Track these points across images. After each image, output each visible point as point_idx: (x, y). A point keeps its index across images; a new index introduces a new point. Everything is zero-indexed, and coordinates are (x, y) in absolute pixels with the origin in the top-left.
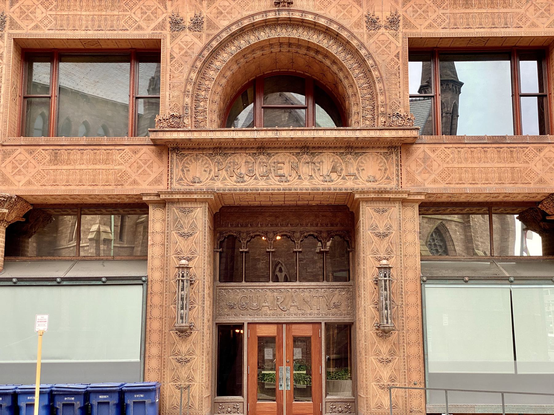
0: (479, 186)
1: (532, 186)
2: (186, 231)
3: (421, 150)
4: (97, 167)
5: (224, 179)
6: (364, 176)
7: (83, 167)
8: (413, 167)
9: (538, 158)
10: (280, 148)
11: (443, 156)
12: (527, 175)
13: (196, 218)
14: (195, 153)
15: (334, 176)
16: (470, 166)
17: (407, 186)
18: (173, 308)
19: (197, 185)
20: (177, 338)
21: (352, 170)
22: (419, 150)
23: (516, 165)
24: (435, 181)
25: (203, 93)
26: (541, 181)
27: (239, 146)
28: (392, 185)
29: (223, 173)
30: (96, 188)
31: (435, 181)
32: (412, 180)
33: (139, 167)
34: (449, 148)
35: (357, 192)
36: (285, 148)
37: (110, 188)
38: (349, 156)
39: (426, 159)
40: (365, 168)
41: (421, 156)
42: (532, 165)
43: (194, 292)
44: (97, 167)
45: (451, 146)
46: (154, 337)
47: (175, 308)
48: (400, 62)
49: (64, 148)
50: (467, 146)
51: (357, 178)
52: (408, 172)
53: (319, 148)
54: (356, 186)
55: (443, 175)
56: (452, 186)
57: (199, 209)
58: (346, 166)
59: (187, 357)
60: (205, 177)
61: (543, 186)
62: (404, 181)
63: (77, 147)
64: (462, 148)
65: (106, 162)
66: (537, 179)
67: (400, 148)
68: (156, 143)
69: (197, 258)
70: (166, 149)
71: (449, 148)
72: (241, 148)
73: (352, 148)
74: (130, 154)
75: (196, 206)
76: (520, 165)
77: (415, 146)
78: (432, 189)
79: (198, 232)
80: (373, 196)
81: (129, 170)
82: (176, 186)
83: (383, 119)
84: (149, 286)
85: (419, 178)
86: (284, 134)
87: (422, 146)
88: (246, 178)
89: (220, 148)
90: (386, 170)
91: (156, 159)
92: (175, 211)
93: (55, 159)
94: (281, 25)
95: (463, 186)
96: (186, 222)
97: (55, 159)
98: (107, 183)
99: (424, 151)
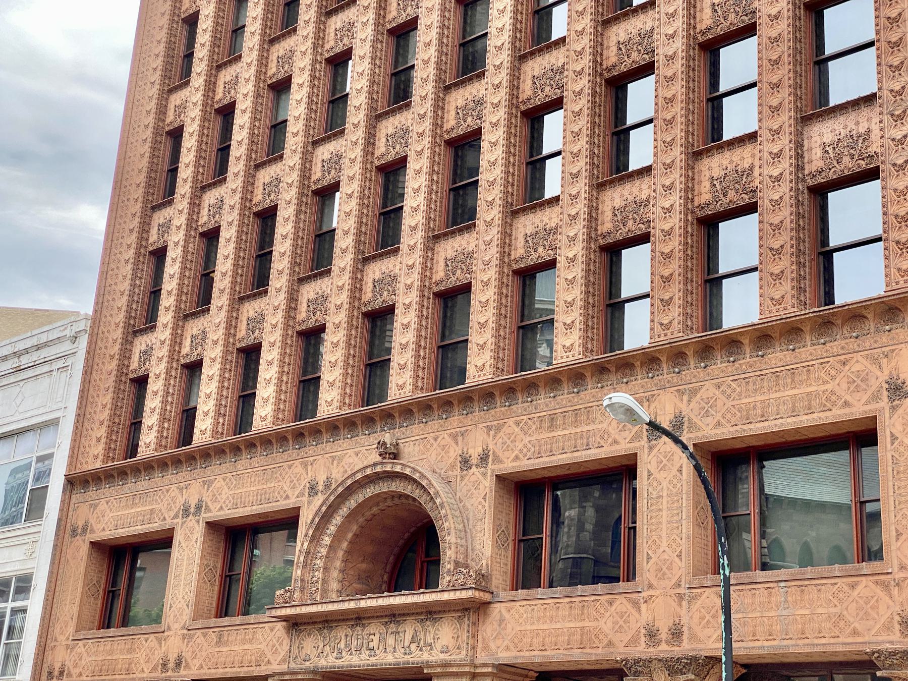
0: (548, 653)
1: (600, 651)
3: (497, 610)
4: (246, 647)
5: (327, 656)
6: (439, 646)
7: (236, 648)
8: (489, 631)
9: (609, 614)
10: (373, 617)
11: (517, 616)
12: (597, 636)
14: (309, 627)
15: (413, 646)
16: (542, 627)
17: (482, 658)
19: (307, 663)
21: (429, 640)
22: (497, 610)
23: (586, 624)
24: (508, 649)
25: (318, 562)
26: (610, 644)
27: (341, 618)
28: (462, 656)
29: (327, 648)
30: (242, 669)
31: (508, 649)
32: (486, 648)
33: (273, 646)
34: (523, 606)
35: (429, 667)
36: (377, 617)
37: (252, 669)
38: (428, 623)
39: (501, 621)
40: (440, 636)
41: (498, 618)
42: (601, 623)
44: (246, 647)
45: (524, 603)
48: (487, 505)
49: (226, 629)
50: (541, 602)
51: (431, 649)
52: (483, 638)
53: (404, 615)
54: (431, 659)
55: (516, 641)
56: (522, 654)
58: (425, 635)
60: (313, 654)
61: (611, 650)
62: (479, 650)
63: (235, 628)
64: (536, 605)
65: (251, 641)
66: (606, 641)
67: (474, 610)
68: (285, 619)
70: (295, 624)
71: (523, 606)
72: (343, 620)
73: (430, 613)
74: (269, 631)
76: (591, 624)
77: (493, 605)
78: (504, 658)
80: (438, 670)
82: (293, 666)
83: (448, 578)
85: (492, 646)
86: (364, 604)
87: (498, 605)
88: (344, 653)
89: (327, 621)
90: (458, 637)
91: (286, 637)
93: (219, 643)
94: (370, 482)
95: (533, 653)
97: (219, 643)
99: (500, 611)
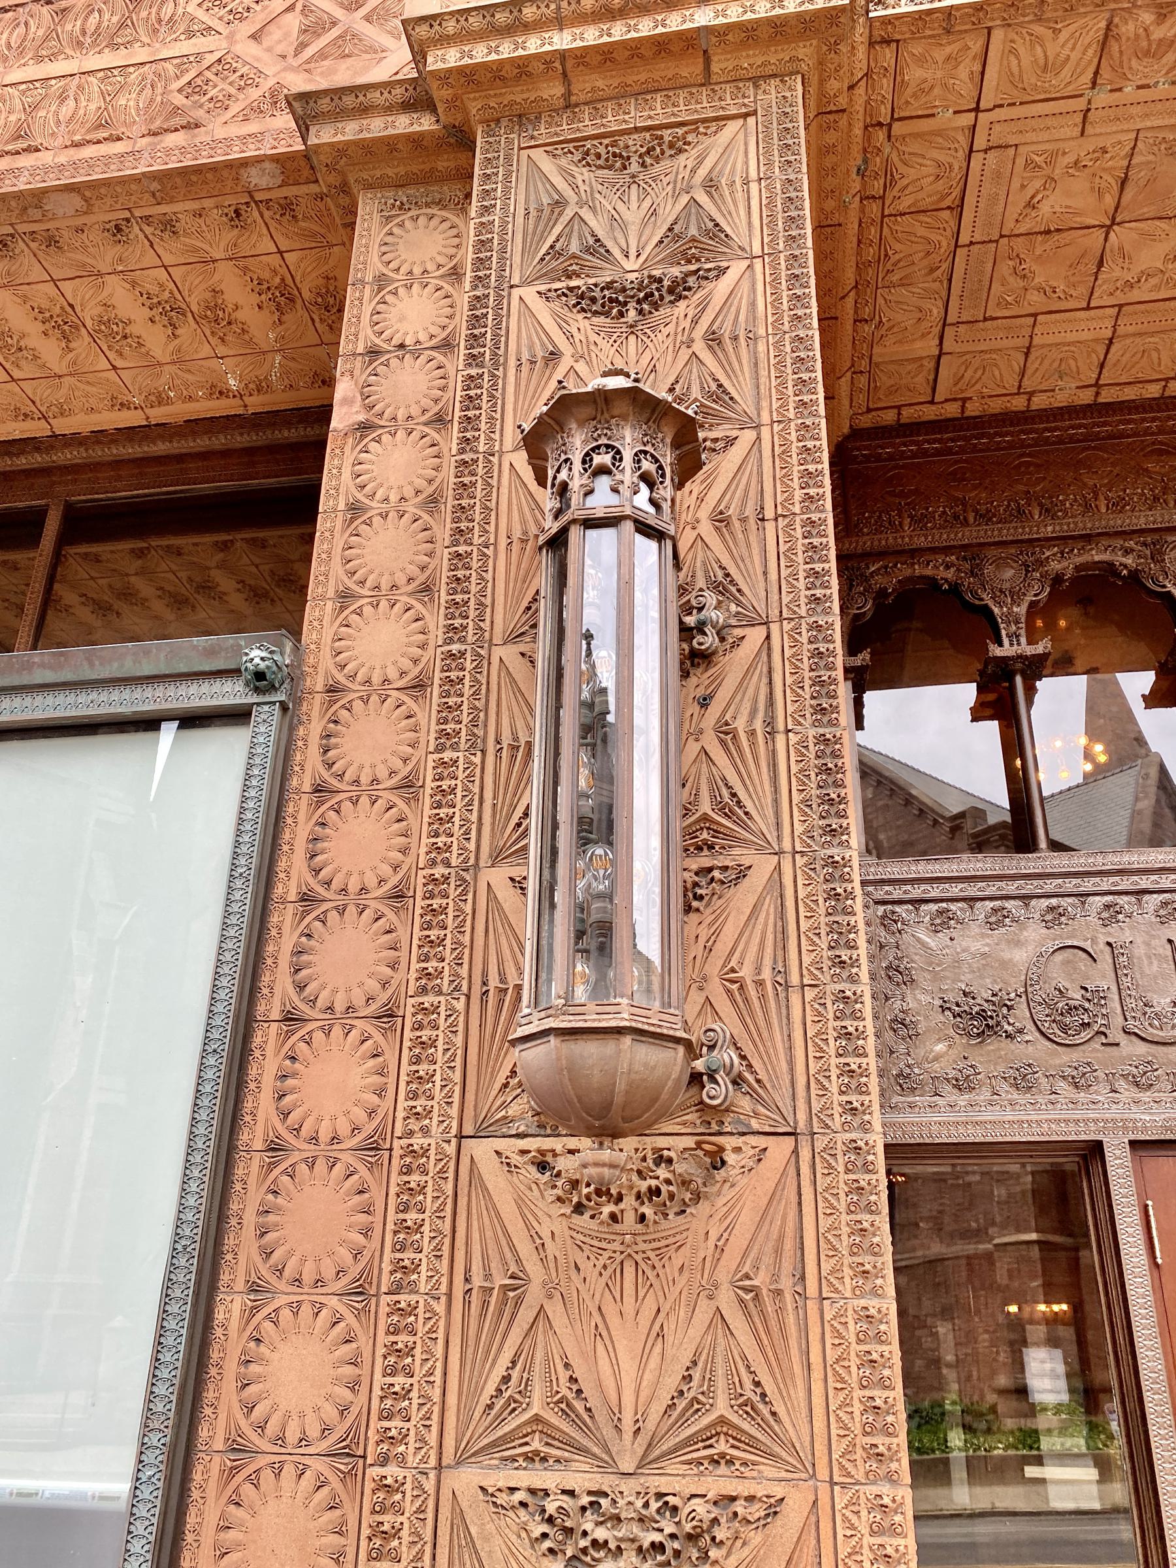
2: (630, 269)
13: (710, 185)
18: (506, 894)
20: (553, 1220)
43: (725, 731)
46: (313, 1219)
47: (519, 884)
57: (733, 126)
59: (676, 1480)
69: (736, 454)
75: (705, 107)
79: (737, 268)
81: (248, 50)
84: (313, 729)
92: (546, 164)
96: (633, 214)
98: (104, 129)
